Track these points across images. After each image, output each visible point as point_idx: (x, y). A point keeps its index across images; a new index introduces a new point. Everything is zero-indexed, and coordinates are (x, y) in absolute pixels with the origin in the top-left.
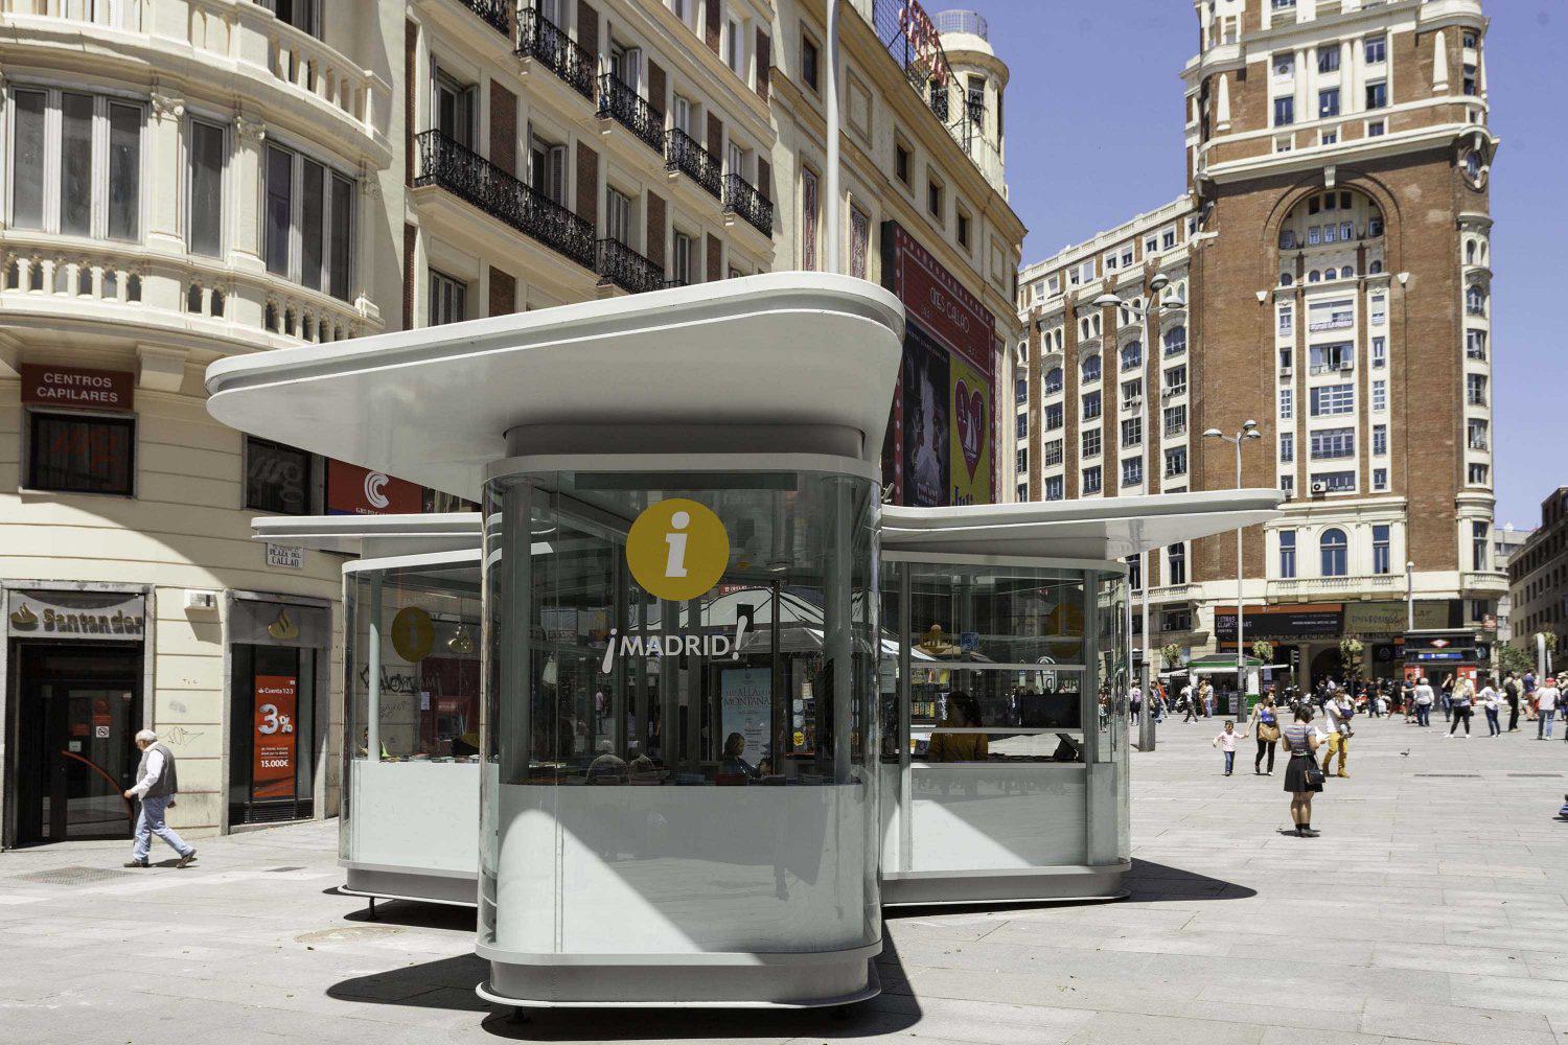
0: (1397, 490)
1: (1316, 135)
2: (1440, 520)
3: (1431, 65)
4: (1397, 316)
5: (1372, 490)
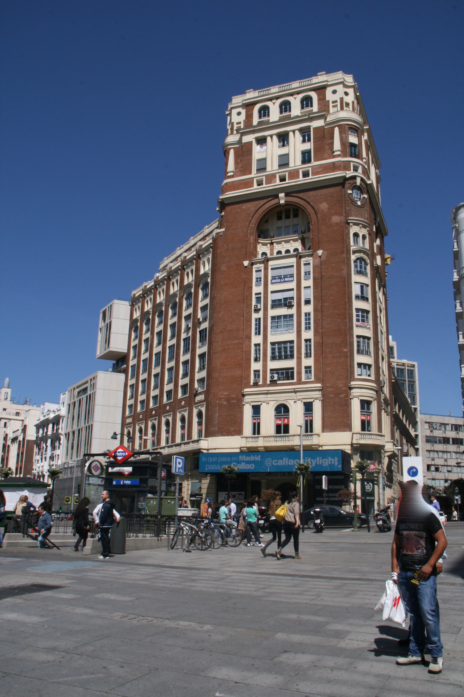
0: (317, 380)
1: (276, 177)
2: (341, 398)
3: (332, 143)
4: (316, 275)
5: (303, 380)
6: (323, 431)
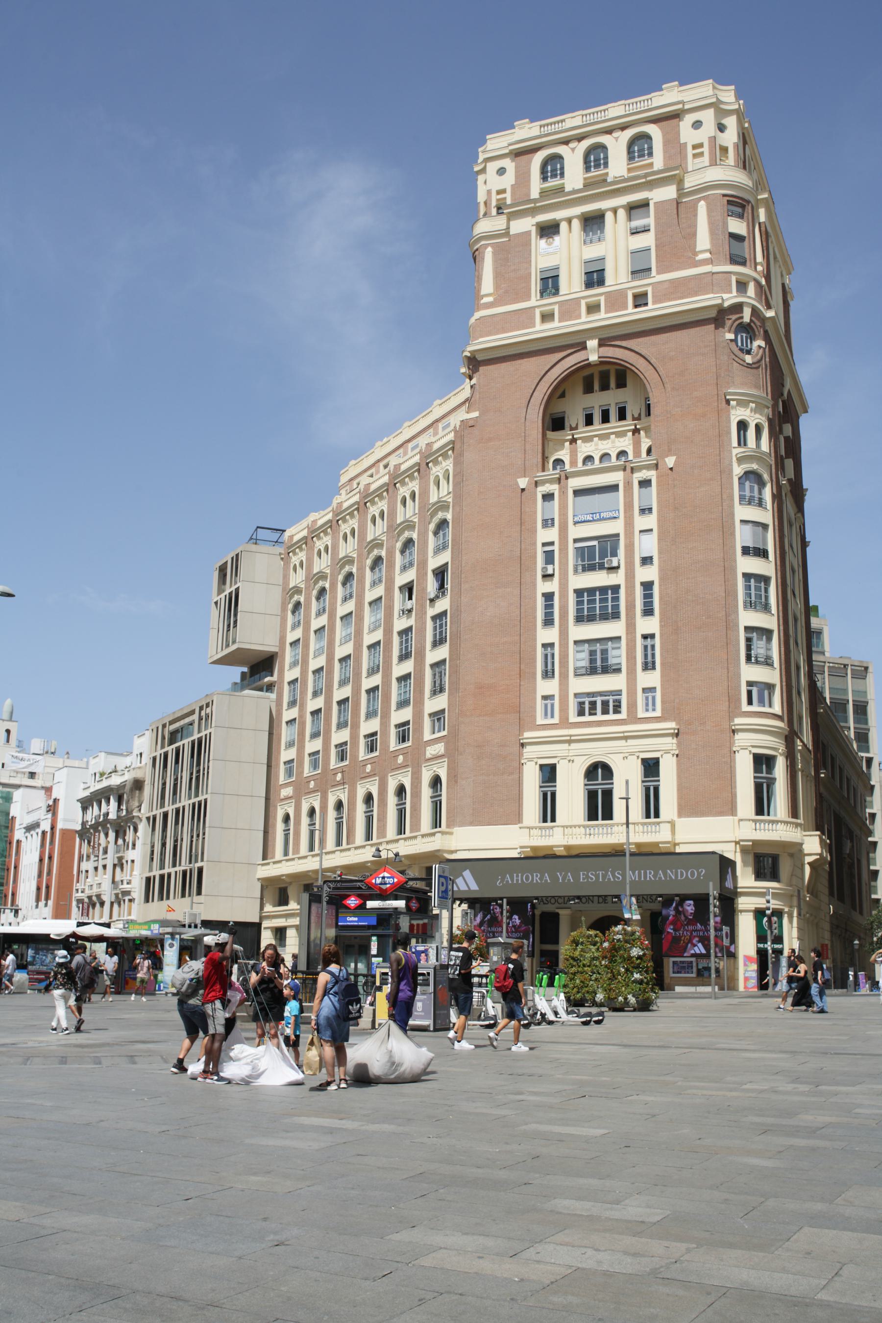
5: (641, 714)
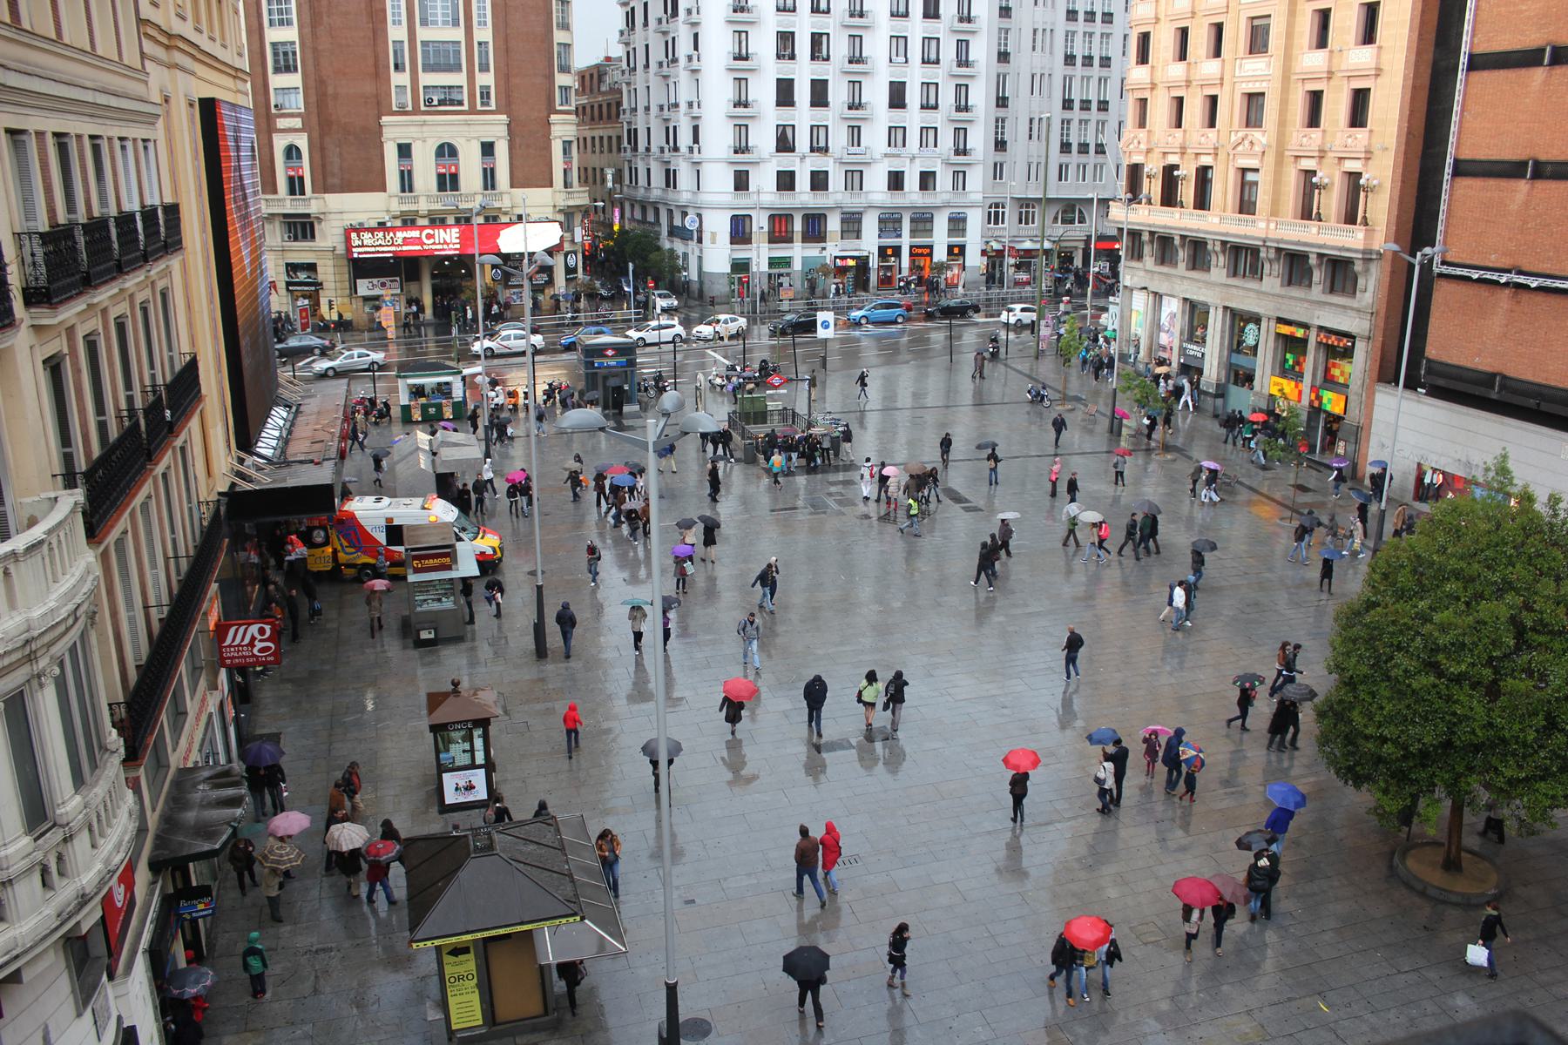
5: (479, 107)
6: (512, 186)
